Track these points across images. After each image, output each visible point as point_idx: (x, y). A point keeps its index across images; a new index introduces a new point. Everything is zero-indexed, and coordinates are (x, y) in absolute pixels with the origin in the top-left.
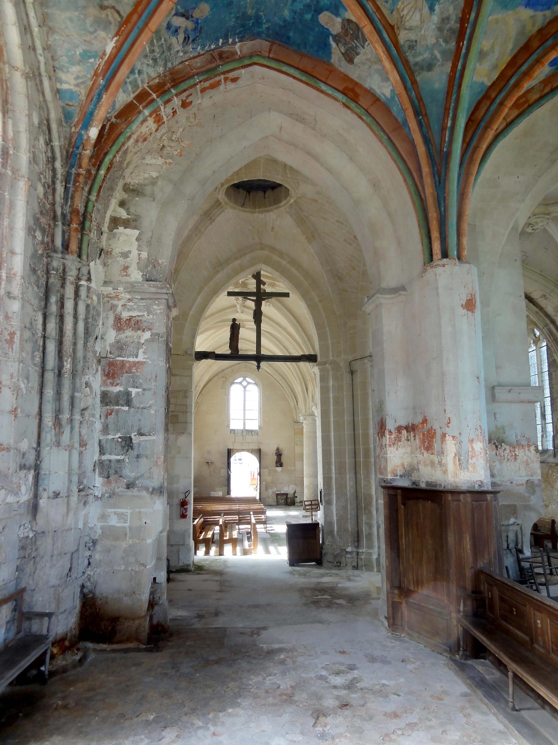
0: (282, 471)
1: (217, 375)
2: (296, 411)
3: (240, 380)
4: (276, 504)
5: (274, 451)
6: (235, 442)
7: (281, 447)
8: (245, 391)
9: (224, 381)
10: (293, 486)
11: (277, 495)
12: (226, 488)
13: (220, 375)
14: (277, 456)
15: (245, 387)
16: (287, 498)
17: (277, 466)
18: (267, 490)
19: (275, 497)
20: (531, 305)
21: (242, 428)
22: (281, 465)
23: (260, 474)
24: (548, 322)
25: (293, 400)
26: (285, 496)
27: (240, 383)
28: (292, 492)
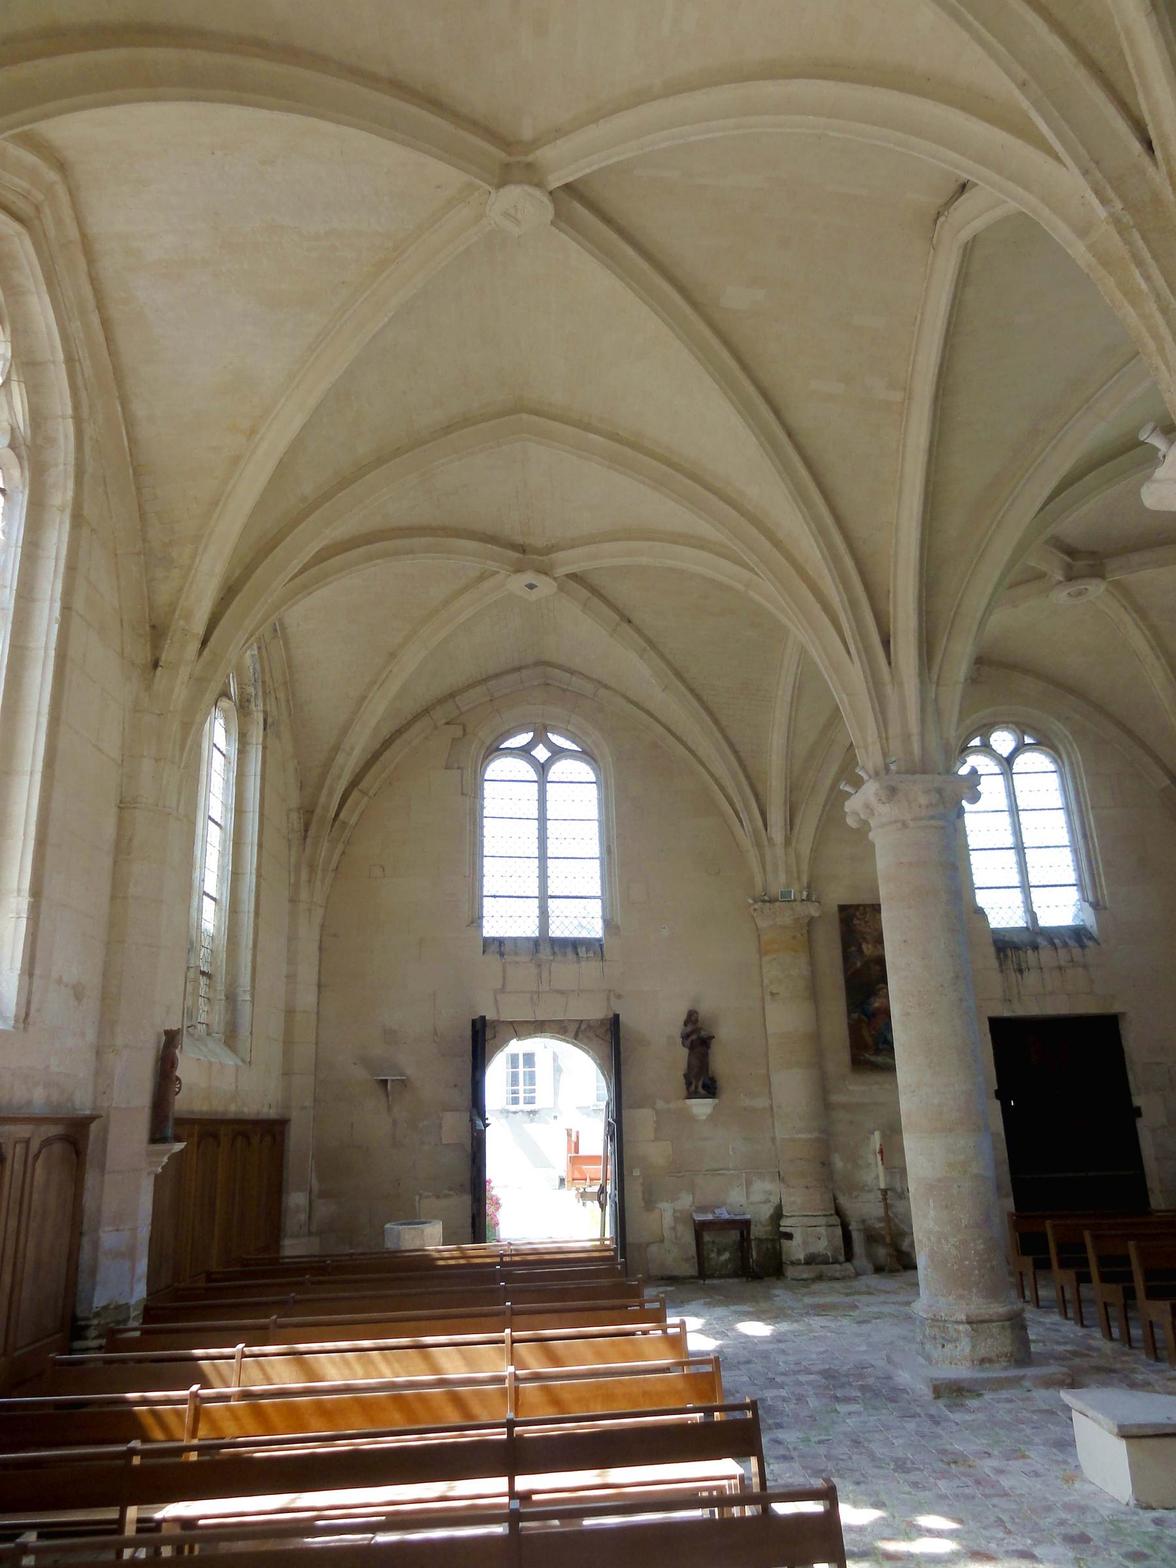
0: (711, 1118)
1: (426, 711)
2: (762, 857)
3: (521, 740)
4: (690, 1269)
5: (676, 1028)
6: (503, 990)
7: (704, 1009)
8: (542, 782)
11: (700, 1229)
12: (467, 1199)
14: (692, 1048)
15: (542, 769)
16: (745, 1239)
17: (692, 1095)
18: (649, 1204)
19: (689, 1237)
23: (617, 1131)
25: (747, 808)
26: (734, 1235)
27: (525, 752)
28: (766, 1211)
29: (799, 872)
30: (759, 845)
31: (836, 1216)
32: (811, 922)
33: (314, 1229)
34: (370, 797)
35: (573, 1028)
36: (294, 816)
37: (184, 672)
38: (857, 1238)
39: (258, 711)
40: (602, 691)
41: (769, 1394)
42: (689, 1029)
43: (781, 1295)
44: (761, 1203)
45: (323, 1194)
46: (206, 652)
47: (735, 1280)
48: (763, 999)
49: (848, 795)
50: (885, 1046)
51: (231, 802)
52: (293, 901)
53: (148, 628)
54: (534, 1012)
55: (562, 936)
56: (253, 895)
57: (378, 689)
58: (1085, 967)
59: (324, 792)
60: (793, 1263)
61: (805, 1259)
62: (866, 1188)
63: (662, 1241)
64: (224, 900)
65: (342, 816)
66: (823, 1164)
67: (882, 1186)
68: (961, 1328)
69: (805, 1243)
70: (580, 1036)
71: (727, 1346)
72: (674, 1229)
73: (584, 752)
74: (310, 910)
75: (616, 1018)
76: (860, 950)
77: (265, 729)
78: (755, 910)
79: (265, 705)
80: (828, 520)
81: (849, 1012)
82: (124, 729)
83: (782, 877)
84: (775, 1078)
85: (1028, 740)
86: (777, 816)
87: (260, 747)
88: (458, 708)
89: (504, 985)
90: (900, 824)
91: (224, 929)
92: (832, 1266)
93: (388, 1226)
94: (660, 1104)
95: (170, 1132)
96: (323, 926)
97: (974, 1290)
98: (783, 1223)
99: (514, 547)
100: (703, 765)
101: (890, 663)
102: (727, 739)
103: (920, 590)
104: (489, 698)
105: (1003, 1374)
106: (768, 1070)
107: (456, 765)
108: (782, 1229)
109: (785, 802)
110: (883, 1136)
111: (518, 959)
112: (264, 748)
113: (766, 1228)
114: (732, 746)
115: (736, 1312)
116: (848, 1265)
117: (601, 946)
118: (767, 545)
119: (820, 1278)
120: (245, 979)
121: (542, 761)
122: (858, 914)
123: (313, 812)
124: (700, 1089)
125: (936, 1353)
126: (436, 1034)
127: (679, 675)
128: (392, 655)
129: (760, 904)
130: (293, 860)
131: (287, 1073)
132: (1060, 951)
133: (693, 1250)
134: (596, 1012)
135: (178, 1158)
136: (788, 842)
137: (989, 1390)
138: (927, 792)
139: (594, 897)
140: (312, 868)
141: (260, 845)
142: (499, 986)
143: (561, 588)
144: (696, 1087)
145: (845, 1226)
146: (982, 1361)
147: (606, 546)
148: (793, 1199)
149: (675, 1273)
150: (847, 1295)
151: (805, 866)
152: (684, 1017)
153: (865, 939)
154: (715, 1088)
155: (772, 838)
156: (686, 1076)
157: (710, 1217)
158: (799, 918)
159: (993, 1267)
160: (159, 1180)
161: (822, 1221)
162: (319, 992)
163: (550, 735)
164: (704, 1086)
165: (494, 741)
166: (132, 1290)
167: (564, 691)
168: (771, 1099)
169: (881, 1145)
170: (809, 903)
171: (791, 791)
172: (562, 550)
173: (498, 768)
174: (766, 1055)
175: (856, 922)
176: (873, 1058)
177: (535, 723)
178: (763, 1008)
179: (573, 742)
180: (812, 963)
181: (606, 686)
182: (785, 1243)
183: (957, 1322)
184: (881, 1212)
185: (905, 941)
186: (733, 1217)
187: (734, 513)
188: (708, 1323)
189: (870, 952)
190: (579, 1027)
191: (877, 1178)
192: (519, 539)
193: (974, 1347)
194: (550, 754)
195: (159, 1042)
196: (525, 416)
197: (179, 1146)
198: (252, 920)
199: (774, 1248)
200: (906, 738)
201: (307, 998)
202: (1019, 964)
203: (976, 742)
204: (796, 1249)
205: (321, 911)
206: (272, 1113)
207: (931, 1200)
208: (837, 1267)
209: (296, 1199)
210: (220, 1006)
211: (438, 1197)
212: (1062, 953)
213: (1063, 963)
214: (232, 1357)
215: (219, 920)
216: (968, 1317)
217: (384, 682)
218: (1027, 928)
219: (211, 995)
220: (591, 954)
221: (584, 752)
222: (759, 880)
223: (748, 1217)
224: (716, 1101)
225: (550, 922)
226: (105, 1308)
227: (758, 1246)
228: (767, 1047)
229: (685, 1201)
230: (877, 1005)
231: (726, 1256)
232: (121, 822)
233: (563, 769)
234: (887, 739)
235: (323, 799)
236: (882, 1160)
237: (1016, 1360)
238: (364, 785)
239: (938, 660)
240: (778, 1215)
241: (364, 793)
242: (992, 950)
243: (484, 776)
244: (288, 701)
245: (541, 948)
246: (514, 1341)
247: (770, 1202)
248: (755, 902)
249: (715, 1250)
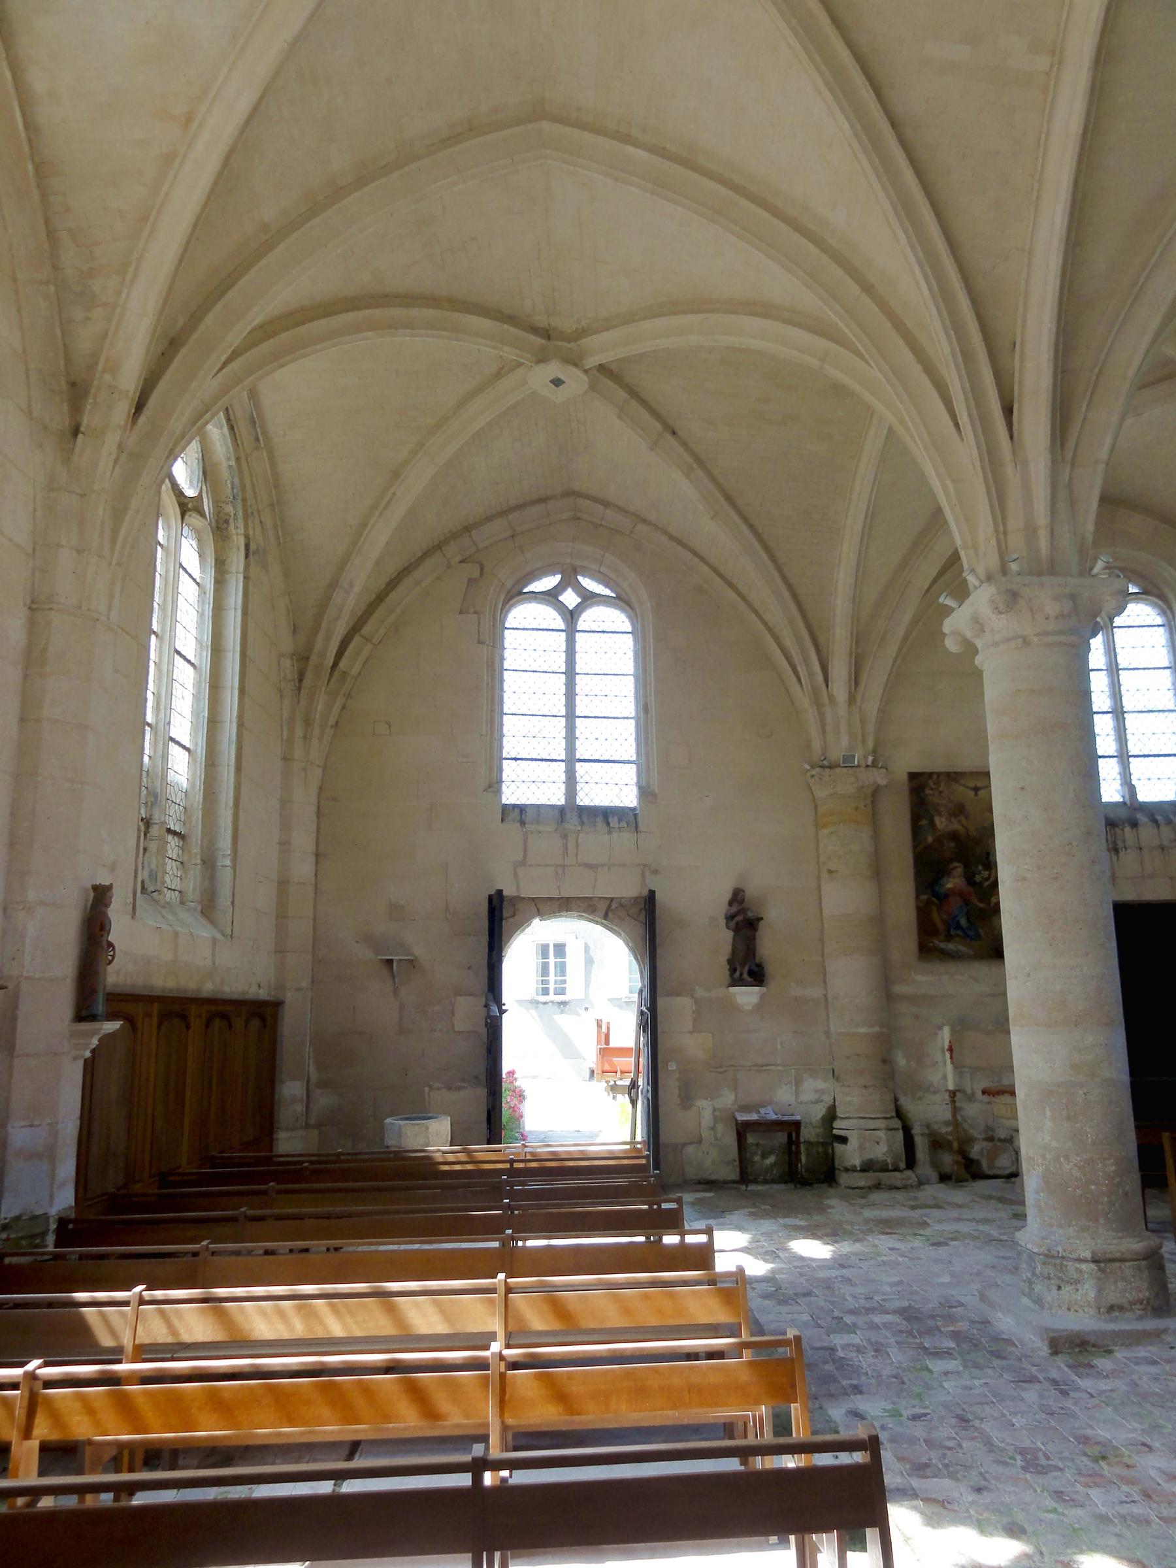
0: (759, 1007)
1: (439, 547)
4: (731, 1173)
6: (523, 863)
7: (751, 891)
8: (571, 631)
9: (470, 580)
10: (820, 1084)
11: (743, 1130)
12: (482, 1093)
13: (452, 549)
14: (737, 930)
15: (571, 616)
17: (735, 982)
18: (686, 1099)
19: (731, 1140)
21: (556, 797)
22: (757, 976)
25: (806, 661)
26: (781, 1138)
27: (551, 597)
28: (819, 1112)
29: (863, 735)
30: (818, 703)
31: (896, 1119)
32: (876, 792)
33: (312, 1121)
34: (374, 644)
35: (603, 906)
36: (287, 663)
37: (111, 440)
38: (921, 1143)
39: (237, 534)
40: (641, 527)
41: (838, 1340)
42: (734, 909)
43: (837, 1208)
44: (812, 1103)
45: (323, 1084)
46: (143, 419)
47: (783, 1186)
48: (819, 878)
49: (949, 611)
50: (959, 932)
51: (207, 639)
52: (286, 759)
53: (64, 385)
54: (559, 887)
55: (592, 804)
56: (233, 746)
57: (381, 514)
59: (321, 636)
60: (847, 1170)
61: (861, 1165)
62: (932, 1089)
63: (700, 1141)
64: (199, 750)
65: (343, 664)
66: (884, 1061)
67: (951, 1087)
68: (1084, 1266)
69: (862, 1147)
70: (610, 915)
71: (780, 1271)
72: (713, 1128)
73: (618, 598)
74: (305, 770)
75: (652, 893)
76: (932, 823)
77: (247, 556)
78: (812, 776)
79: (246, 527)
80: (940, 245)
81: (917, 897)
82: (35, 510)
83: (845, 741)
86: (840, 670)
87: (241, 577)
88: (475, 544)
89: (525, 856)
90: (1020, 640)
91: (199, 784)
92: (892, 1173)
93: (388, 1120)
94: (700, 992)
95: (100, 1008)
96: (321, 788)
97: (1102, 1221)
98: (836, 1124)
99: (535, 330)
100: (755, 611)
101: (1011, 437)
102: (784, 578)
103: (1057, 344)
104: (509, 533)
105: (1138, 1326)
106: (823, 956)
107: (472, 610)
108: (835, 1132)
109: (851, 654)
110: (953, 1032)
111: (541, 828)
112: (246, 578)
113: (818, 1131)
114: (790, 587)
115: (785, 1226)
116: (909, 1173)
117: (635, 815)
118: (855, 289)
119: (878, 1186)
120: (225, 842)
121: (571, 608)
122: (931, 782)
123: (308, 658)
124: (746, 976)
125: (1051, 1296)
126: (447, 910)
127: (729, 498)
128: (396, 474)
129: (818, 769)
130: (286, 714)
131: (280, 950)
132: (1162, 828)
133: (734, 1152)
134: (628, 888)
135: (107, 1039)
136: (852, 700)
137: (1122, 1345)
138: (1057, 598)
139: (629, 762)
140: (308, 723)
141: (242, 691)
142: (520, 857)
143: (593, 387)
144: (741, 974)
146: (1111, 1308)
147: (647, 325)
148: (849, 1099)
149: (713, 1177)
150: (913, 1208)
151: (871, 728)
152: (728, 896)
154: (763, 976)
155: (833, 696)
156: (729, 961)
157: (754, 1117)
158: (863, 787)
159: (1126, 1194)
160: (90, 1067)
162: (317, 862)
163: (580, 578)
164: (751, 973)
165: (518, 582)
166: (51, 1198)
167: (596, 526)
168: (826, 988)
169: (950, 1042)
170: (875, 770)
171: (857, 642)
172: (597, 332)
173: (522, 615)
174: (822, 940)
175: (928, 791)
176: (942, 945)
177: (563, 565)
178: (819, 887)
179: (607, 586)
180: (876, 836)
181: (645, 521)
182: (839, 1147)
183: (1079, 1260)
184: (948, 1115)
185: (1022, 788)
186: (780, 1118)
187: (812, 248)
188: (754, 1241)
189: (943, 826)
190: (610, 906)
191: (945, 1077)
192: (541, 321)
193: (1100, 1291)
194: (579, 600)
195: (87, 901)
196: (546, 125)
197: (112, 1026)
198: (232, 775)
199: (826, 1152)
200: (1031, 531)
201: (303, 868)
202: (1115, 843)
204: (851, 1154)
205: (318, 772)
206: (263, 994)
207: (1047, 1109)
208: (897, 1174)
209: (291, 1090)
210: (196, 872)
211: (449, 1089)
212: (1165, 829)
213: (1165, 843)
214: (126, 1303)
215: (194, 774)
216: (1094, 1253)
217: (385, 508)
218: (1124, 803)
219: (185, 859)
220: (624, 824)
221: (618, 598)
222: (817, 745)
223: (798, 1118)
224: (764, 989)
225: (578, 788)
226: (17, 1219)
227: (807, 1149)
228: (822, 930)
229: (727, 1099)
230: (949, 886)
231: (771, 1160)
232: (32, 626)
233: (592, 617)
234: (1005, 533)
235: (319, 645)
236: (951, 1058)
237: (1153, 1308)
238: (367, 629)
239: (1074, 430)
240: (831, 1115)
241: (367, 639)
243: (504, 624)
244: (275, 527)
245: (568, 816)
246: (509, 1290)
247: (822, 1101)
248: (813, 767)
249: (760, 1153)
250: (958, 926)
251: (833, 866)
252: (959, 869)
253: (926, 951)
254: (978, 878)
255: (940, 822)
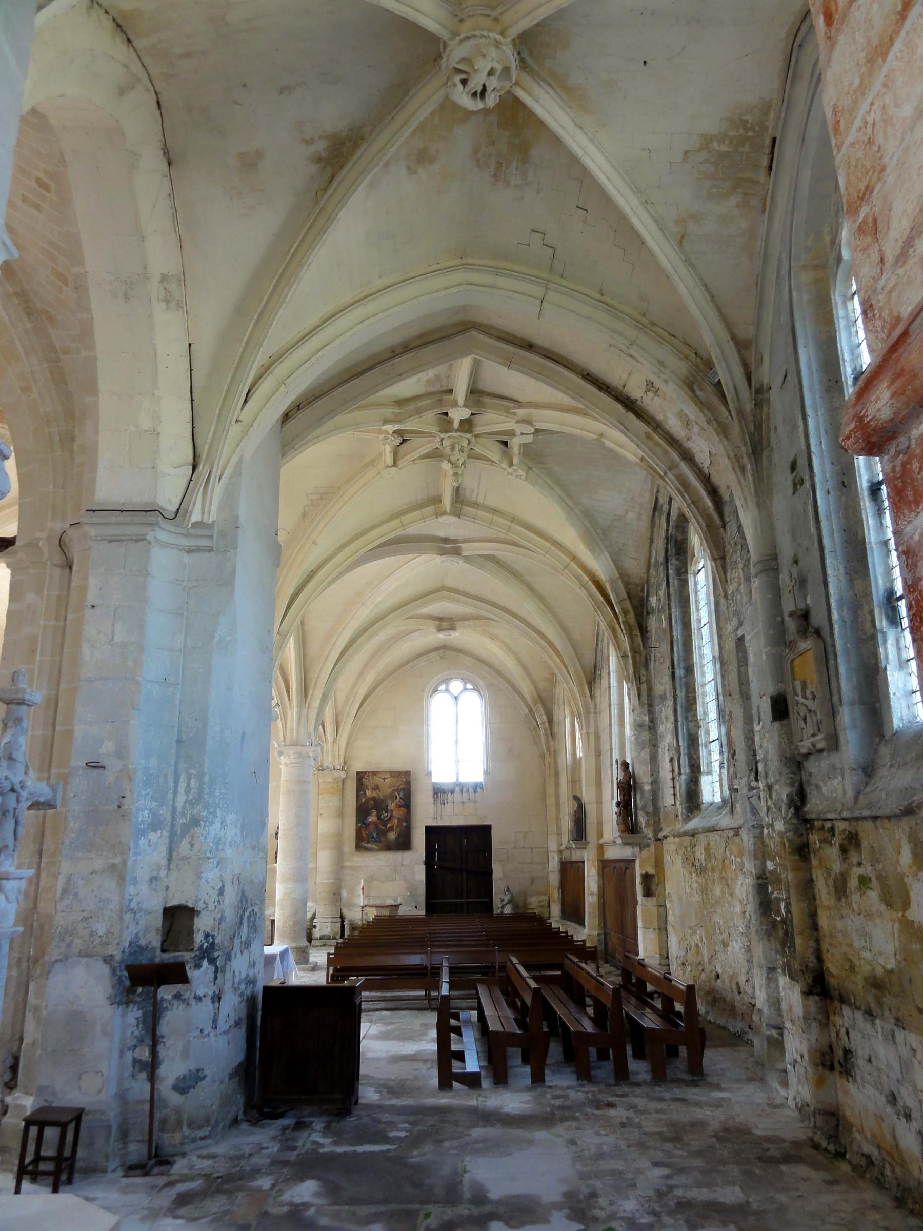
20: (631, 416)
24: (676, 457)
58: (475, 802)
69: (320, 930)
76: (365, 793)
81: (357, 824)
83: (330, 758)
84: (319, 855)
85: (469, 686)
86: (330, 728)
110: (365, 881)
136: (335, 741)
145: (343, 922)
151: (342, 753)
153: (368, 788)
161: (330, 920)
176: (366, 845)
200: (292, 730)
203: (443, 687)
230: (370, 820)
242: (431, 793)
250: (373, 837)
251: (321, 812)
252: (375, 813)
253: (359, 847)
254: (382, 817)
255: (369, 793)
